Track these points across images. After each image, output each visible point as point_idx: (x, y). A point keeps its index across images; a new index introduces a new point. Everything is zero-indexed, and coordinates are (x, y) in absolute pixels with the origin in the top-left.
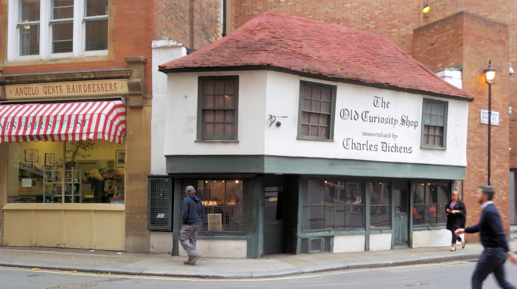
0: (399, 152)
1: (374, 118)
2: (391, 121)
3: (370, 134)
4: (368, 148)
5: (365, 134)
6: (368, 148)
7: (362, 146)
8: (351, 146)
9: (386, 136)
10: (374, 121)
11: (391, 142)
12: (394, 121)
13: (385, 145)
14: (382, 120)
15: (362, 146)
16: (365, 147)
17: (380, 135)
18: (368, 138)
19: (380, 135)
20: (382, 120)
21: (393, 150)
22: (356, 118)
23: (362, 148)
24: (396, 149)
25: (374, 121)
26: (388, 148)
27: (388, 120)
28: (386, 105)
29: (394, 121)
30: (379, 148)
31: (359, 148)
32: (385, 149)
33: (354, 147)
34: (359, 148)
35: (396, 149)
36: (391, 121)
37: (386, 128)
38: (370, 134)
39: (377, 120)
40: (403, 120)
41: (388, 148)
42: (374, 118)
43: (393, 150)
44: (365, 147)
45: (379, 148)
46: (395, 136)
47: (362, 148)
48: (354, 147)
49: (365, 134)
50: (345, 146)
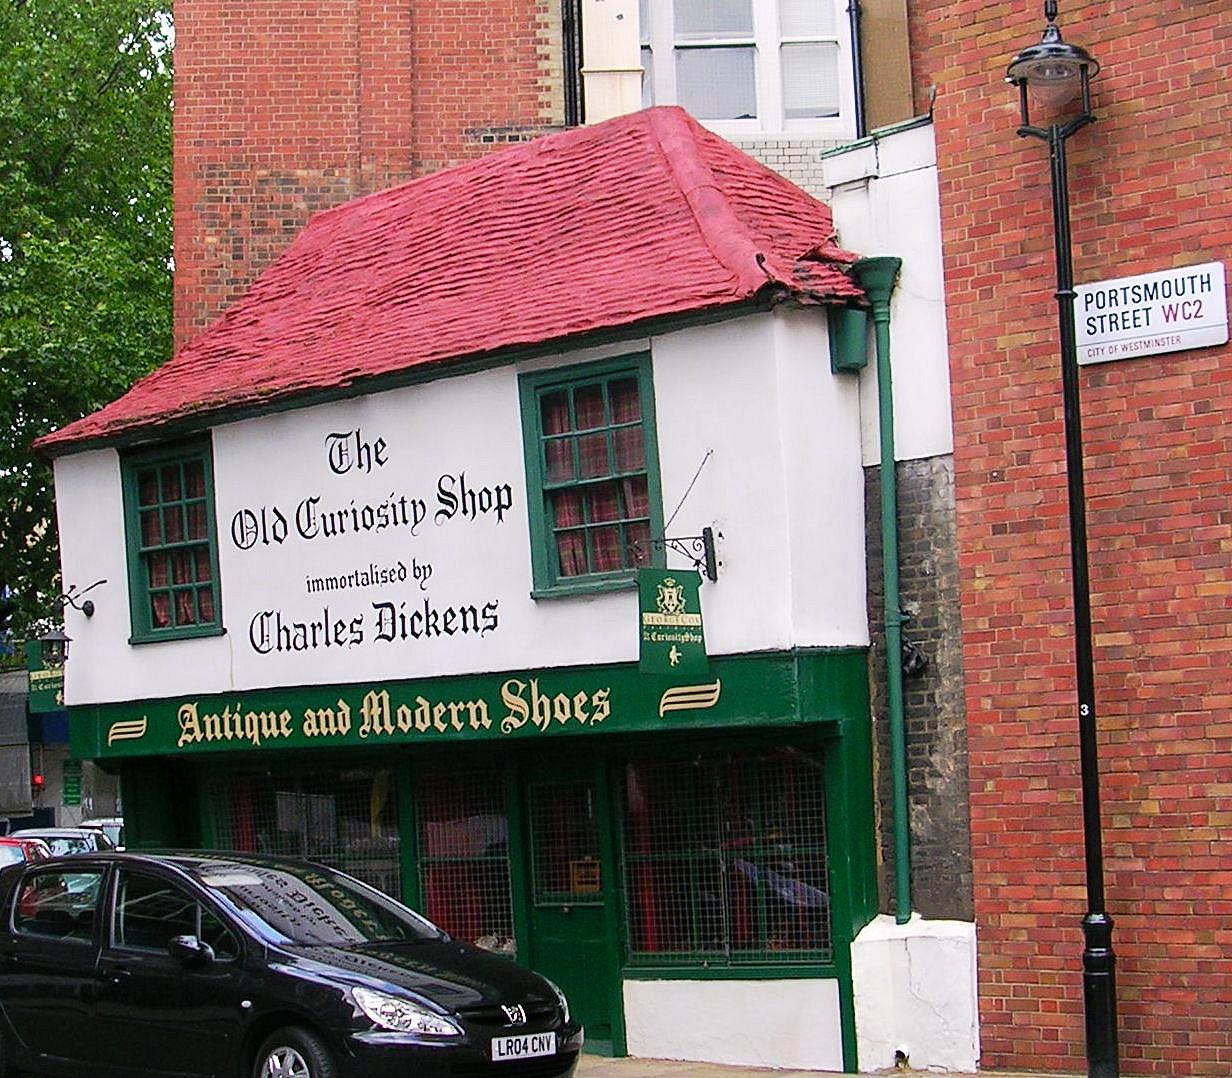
0: (444, 634)
1: (337, 517)
2: (403, 512)
3: (332, 583)
4: (332, 639)
5: (315, 585)
6: (332, 639)
7: (309, 630)
8: (274, 642)
9: (387, 577)
10: (338, 529)
11: (407, 596)
12: (409, 507)
13: (387, 612)
14: (367, 518)
15: (309, 630)
16: (321, 635)
17: (370, 578)
18: (325, 597)
19: (370, 578)
20: (367, 518)
21: (420, 626)
22: (280, 534)
23: (310, 642)
24: (431, 622)
25: (338, 529)
26: (399, 621)
27: (389, 511)
28: (373, 454)
29: (409, 507)
30: (370, 629)
31: (300, 644)
32: (388, 630)
33: (284, 644)
34: (300, 643)
35: (431, 622)
36: (403, 512)
37: (387, 546)
38: (332, 583)
39: (348, 522)
40: (446, 497)
41: (399, 621)
42: (337, 517)
43: (420, 626)
44: (321, 635)
45: (370, 629)
46: (422, 572)
47: (310, 642)
48: (284, 644)
49: (315, 585)
50: (258, 643)
